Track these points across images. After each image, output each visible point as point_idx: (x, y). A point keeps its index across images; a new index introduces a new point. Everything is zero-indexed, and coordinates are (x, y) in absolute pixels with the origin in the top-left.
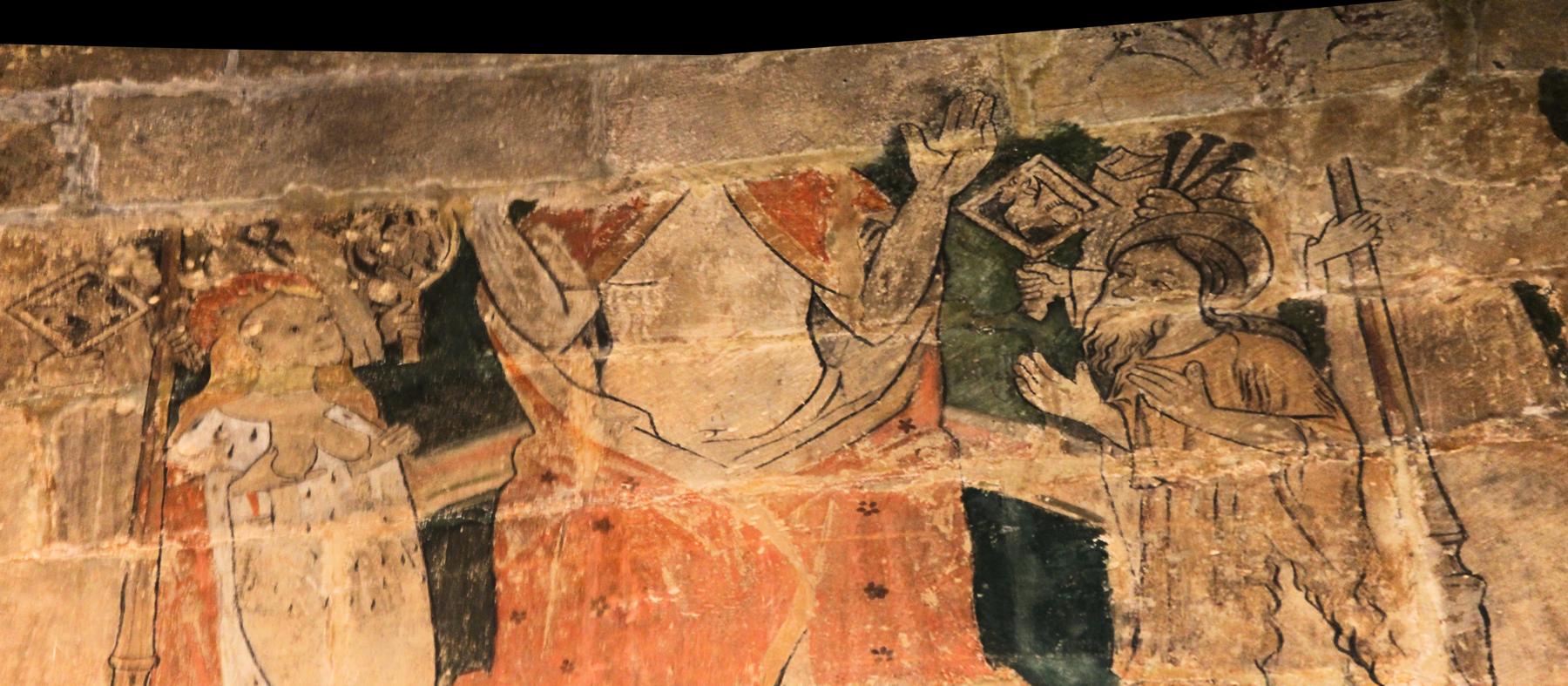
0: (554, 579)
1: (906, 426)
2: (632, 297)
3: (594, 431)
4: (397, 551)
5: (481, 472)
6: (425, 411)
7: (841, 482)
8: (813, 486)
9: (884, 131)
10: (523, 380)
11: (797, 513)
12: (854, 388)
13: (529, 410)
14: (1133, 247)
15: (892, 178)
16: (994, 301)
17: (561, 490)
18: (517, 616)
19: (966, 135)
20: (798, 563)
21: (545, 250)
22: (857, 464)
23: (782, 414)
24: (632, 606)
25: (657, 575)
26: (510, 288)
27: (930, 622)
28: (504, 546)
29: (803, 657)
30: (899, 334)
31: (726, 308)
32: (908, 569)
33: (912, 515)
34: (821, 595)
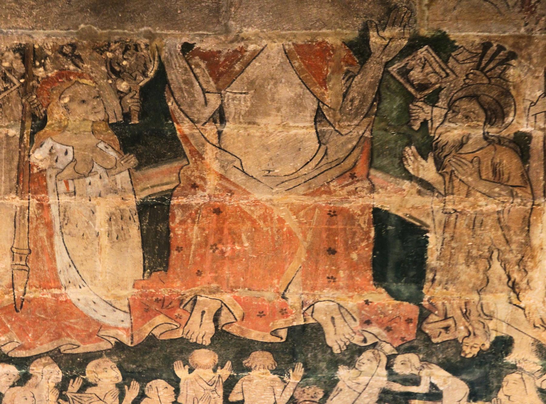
0: (195, 233)
1: (353, 176)
3: (215, 166)
4: (128, 214)
5: (166, 180)
6: (141, 148)
7: (322, 200)
8: (309, 201)
9: (359, 23)
10: (185, 137)
11: (302, 213)
12: (332, 156)
13: (187, 153)
14: (460, 98)
15: (360, 49)
16: (398, 119)
17: (200, 193)
18: (179, 249)
19: (397, 30)
20: (300, 236)
21: (197, 71)
22: (329, 193)
23: (299, 165)
24: (228, 249)
25: (240, 237)
26: (181, 89)
27: (353, 266)
28: (174, 217)
29: (298, 279)
30: (354, 130)
31: (278, 110)
32: (346, 243)
33: (351, 218)
34: (309, 251)
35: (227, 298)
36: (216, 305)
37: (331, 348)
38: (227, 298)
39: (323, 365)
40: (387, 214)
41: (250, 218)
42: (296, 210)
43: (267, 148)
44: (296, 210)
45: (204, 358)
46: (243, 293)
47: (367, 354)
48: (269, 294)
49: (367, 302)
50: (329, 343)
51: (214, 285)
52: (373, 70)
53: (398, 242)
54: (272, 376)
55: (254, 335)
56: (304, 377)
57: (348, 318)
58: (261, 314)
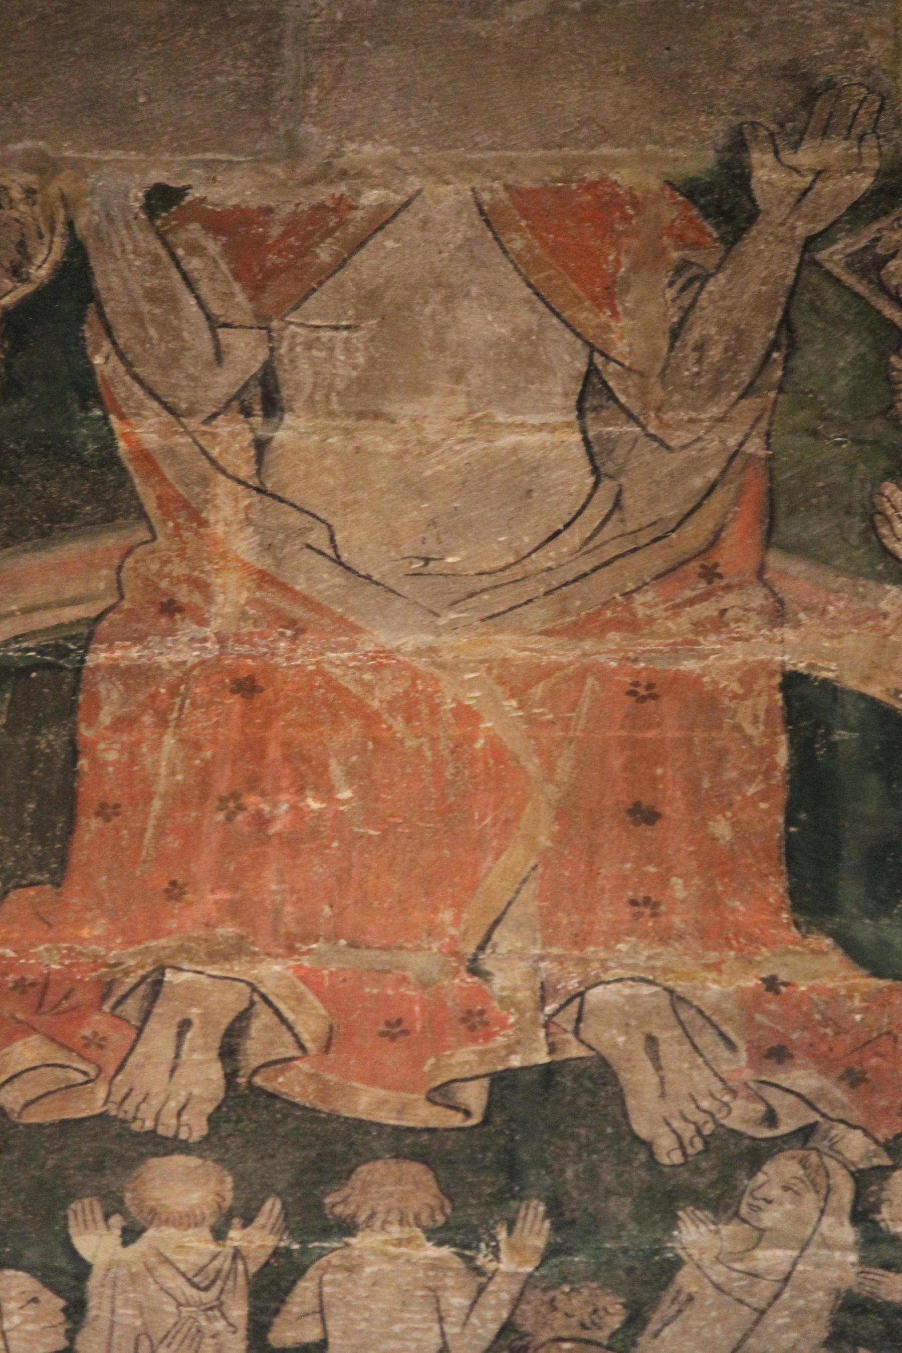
0: (165, 759)
1: (710, 574)
2: (320, 346)
3: (244, 545)
5: (72, 590)
7: (607, 651)
8: (563, 654)
10: (144, 457)
11: (538, 691)
12: (638, 511)
13: (151, 505)
15: (724, 203)
17: (188, 629)
18: (106, 811)
20: (533, 765)
21: (194, 264)
23: (528, 541)
24: (281, 811)
26: (137, 317)
27: (717, 864)
28: (96, 705)
29: (528, 905)
30: (711, 436)
31: (458, 376)
32: (692, 785)
33: (706, 704)
34: (562, 814)
35: (272, 972)
36: (232, 1001)
37: (647, 1145)
38: (272, 972)
39: (621, 1207)
40: (831, 690)
41: (359, 710)
42: (515, 682)
43: (420, 490)
44: (515, 682)
45: (184, 1187)
46: (328, 959)
47: (783, 1168)
48: (422, 961)
49: (771, 984)
50: (642, 1128)
51: (228, 930)
52: (767, 258)
53: (874, 780)
54: (431, 1251)
55: (367, 1103)
56: (552, 1252)
57: (707, 1039)
58: (395, 1029)
